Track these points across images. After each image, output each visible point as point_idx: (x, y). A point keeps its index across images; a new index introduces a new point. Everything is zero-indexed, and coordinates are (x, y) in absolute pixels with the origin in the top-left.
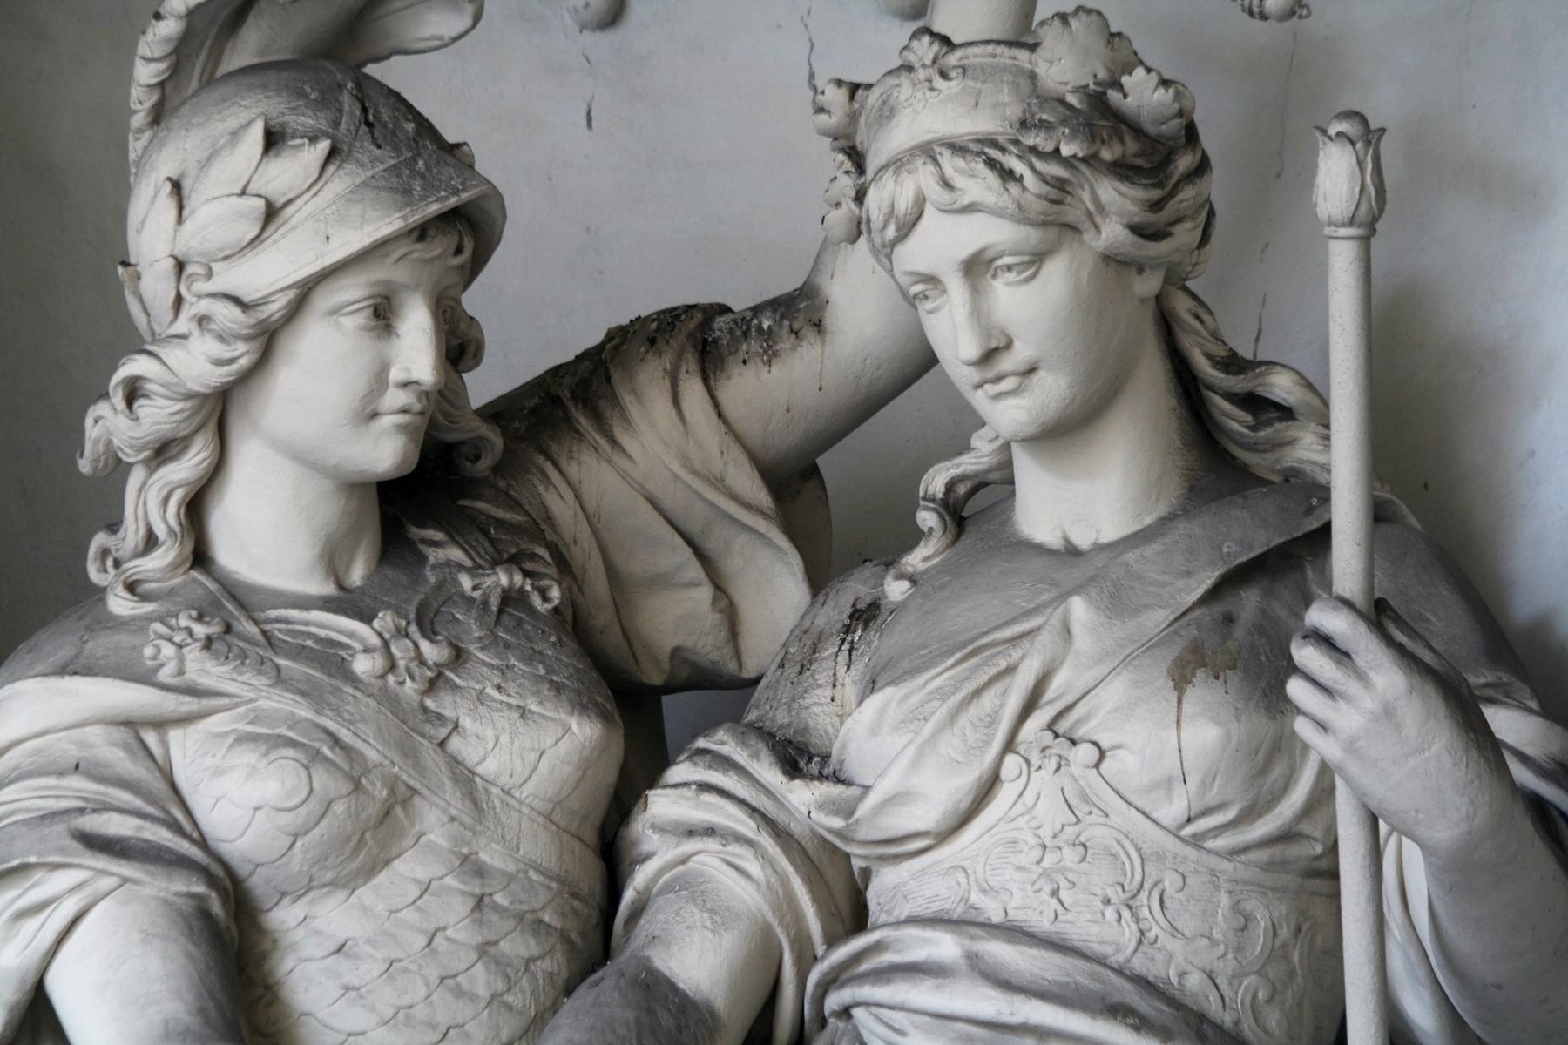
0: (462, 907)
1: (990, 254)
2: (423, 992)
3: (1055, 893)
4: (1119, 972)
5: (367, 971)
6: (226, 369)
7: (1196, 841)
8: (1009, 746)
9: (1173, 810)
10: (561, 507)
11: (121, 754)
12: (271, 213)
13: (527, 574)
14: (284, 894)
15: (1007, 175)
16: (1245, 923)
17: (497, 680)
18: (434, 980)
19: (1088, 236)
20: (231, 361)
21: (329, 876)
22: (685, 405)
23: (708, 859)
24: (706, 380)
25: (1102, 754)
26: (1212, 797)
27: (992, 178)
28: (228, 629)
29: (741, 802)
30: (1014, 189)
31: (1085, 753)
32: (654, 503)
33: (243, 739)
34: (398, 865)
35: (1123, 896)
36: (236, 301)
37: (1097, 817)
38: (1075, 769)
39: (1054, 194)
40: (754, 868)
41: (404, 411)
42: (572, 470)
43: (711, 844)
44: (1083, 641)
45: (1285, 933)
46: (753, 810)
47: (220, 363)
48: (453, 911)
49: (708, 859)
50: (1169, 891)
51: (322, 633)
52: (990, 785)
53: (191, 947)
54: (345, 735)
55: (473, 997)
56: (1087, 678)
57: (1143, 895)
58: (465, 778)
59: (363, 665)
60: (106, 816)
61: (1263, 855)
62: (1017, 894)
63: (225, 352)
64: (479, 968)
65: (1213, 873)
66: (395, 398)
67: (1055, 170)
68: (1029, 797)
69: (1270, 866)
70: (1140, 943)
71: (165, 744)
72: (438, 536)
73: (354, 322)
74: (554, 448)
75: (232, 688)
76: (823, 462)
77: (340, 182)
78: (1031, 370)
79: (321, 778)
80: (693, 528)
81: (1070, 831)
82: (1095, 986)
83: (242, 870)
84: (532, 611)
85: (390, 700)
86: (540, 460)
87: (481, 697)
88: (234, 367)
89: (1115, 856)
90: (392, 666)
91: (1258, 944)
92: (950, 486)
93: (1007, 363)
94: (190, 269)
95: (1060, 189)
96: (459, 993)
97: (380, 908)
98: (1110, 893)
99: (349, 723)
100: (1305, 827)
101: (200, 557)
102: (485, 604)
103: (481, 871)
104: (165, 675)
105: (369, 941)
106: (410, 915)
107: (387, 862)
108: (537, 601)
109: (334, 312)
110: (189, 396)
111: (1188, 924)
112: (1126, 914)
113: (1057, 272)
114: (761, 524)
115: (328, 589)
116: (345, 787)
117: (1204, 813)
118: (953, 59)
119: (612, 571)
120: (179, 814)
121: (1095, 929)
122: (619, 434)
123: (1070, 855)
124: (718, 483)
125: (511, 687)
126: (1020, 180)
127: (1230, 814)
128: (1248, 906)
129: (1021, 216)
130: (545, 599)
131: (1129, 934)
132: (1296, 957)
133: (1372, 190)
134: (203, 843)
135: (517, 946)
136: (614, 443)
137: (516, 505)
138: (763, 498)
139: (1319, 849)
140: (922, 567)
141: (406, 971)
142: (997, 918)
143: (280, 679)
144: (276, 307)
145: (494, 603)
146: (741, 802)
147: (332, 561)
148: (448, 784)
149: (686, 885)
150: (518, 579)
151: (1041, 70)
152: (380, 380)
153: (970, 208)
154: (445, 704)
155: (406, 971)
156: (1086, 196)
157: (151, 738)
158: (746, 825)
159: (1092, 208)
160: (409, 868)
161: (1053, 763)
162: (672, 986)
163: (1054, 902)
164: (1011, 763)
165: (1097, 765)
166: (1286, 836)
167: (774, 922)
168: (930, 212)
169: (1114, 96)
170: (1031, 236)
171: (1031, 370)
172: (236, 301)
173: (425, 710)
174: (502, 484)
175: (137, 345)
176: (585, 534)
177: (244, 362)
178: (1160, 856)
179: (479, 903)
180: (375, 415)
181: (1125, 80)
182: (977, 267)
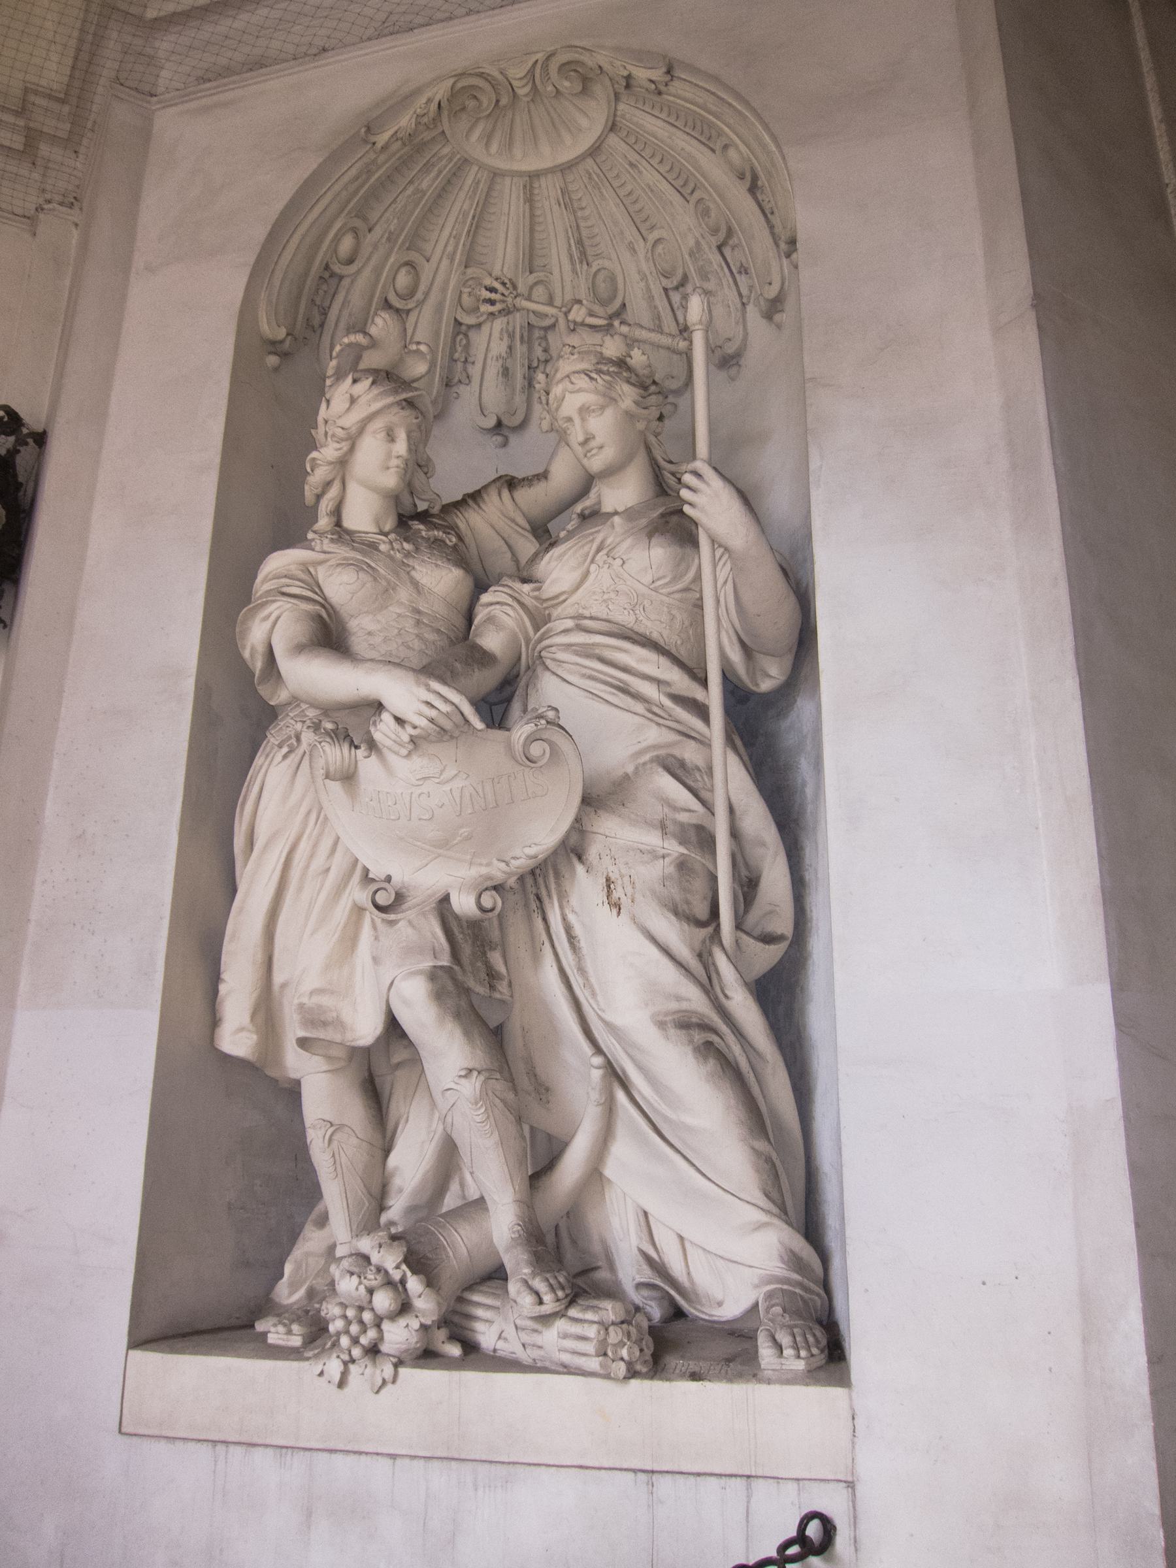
0: (411, 622)
1: (587, 406)
2: (395, 646)
3: (607, 606)
4: (628, 629)
5: (378, 640)
6: (339, 452)
7: (655, 590)
8: (592, 561)
9: (647, 579)
10: (462, 525)
11: (300, 572)
12: (353, 400)
13: (444, 532)
14: (352, 616)
15: (591, 378)
16: (673, 618)
17: (429, 555)
18: (400, 643)
19: (620, 403)
20: (340, 449)
21: (366, 609)
22: (503, 499)
23: (496, 610)
24: (510, 491)
25: (624, 562)
26: (661, 574)
27: (587, 378)
28: (340, 537)
29: (505, 593)
30: (594, 382)
31: (618, 562)
32: (493, 527)
33: (338, 565)
34: (391, 608)
35: (631, 607)
36: (343, 428)
37: (622, 582)
38: (615, 567)
39: (608, 386)
40: (511, 612)
41: (398, 467)
42: (466, 515)
43: (498, 607)
44: (618, 529)
45: (687, 623)
46: (511, 596)
47: (337, 450)
48: (409, 625)
49: (496, 610)
50: (647, 605)
51: (371, 540)
52: (588, 573)
53: (312, 623)
54: (373, 565)
55: (414, 650)
56: (618, 540)
57: (637, 606)
58: (416, 585)
59: (383, 547)
60: (290, 588)
61: (677, 596)
62: (594, 608)
63: (338, 446)
64: (416, 640)
65: (662, 601)
66: (395, 462)
67: (607, 378)
68: (599, 577)
69: (681, 601)
70: (636, 622)
71: (316, 571)
72: (417, 523)
73: (382, 435)
74: (461, 509)
75: (337, 551)
76: (549, 526)
77: (376, 391)
78: (601, 447)
79: (362, 575)
80: (506, 536)
81: (612, 587)
82: (620, 632)
83: (338, 607)
84: (446, 544)
85: (392, 558)
86: (456, 511)
87: (423, 561)
88: (341, 451)
89: (628, 594)
90: (393, 549)
91: (677, 625)
92: (582, 510)
93: (593, 444)
94: (330, 422)
95: (610, 386)
96: (409, 648)
97: (383, 621)
98: (626, 606)
99: (373, 561)
100: (693, 587)
101: (338, 524)
102: (429, 539)
103: (419, 612)
104: (317, 548)
105: (379, 631)
106: (394, 624)
107: (387, 607)
108: (448, 541)
109: (374, 432)
110: (330, 463)
111: (653, 617)
112: (631, 612)
113: (609, 412)
114: (526, 534)
115: (378, 531)
116: (370, 579)
117: (658, 579)
118: (576, 350)
119: (477, 546)
120: (317, 590)
121: (620, 617)
122: (481, 505)
123: (613, 595)
124: (513, 521)
125: (434, 558)
126: (596, 380)
127: (667, 580)
128: (674, 612)
129: (596, 391)
130: (451, 541)
131: (632, 619)
132: (691, 633)
133: (707, 311)
134: (325, 599)
135: (431, 636)
136: (479, 506)
137: (446, 521)
138: (527, 526)
139: (698, 595)
140: (571, 528)
141: (390, 640)
142: (588, 615)
143: (354, 549)
144: (354, 430)
145: (432, 540)
146: (505, 593)
147: (377, 522)
148: (409, 584)
149: (490, 619)
150: (441, 533)
151: (604, 351)
152: (389, 456)
153: (579, 391)
154: (410, 562)
155: (390, 640)
156: (618, 388)
157: (312, 570)
158: (509, 601)
159: (620, 393)
160: (395, 609)
161: (607, 565)
162: (481, 648)
163: (607, 609)
164: (593, 567)
165: (622, 566)
166: (686, 590)
167: (518, 631)
168: (567, 395)
169: (628, 359)
170: (601, 400)
171: (601, 447)
172: (343, 428)
173: (403, 562)
174: (442, 515)
175: (316, 448)
176: (469, 533)
177: (345, 449)
178: (643, 595)
179: (418, 623)
180: (388, 468)
181: (632, 353)
182: (584, 410)
